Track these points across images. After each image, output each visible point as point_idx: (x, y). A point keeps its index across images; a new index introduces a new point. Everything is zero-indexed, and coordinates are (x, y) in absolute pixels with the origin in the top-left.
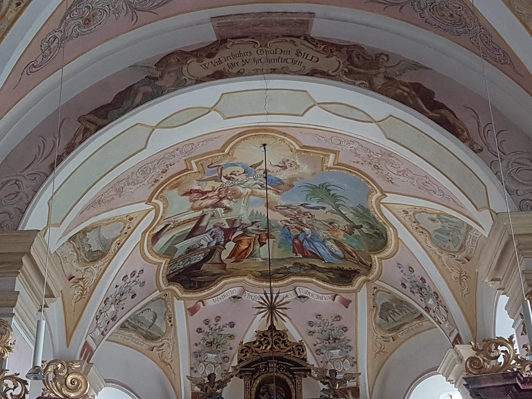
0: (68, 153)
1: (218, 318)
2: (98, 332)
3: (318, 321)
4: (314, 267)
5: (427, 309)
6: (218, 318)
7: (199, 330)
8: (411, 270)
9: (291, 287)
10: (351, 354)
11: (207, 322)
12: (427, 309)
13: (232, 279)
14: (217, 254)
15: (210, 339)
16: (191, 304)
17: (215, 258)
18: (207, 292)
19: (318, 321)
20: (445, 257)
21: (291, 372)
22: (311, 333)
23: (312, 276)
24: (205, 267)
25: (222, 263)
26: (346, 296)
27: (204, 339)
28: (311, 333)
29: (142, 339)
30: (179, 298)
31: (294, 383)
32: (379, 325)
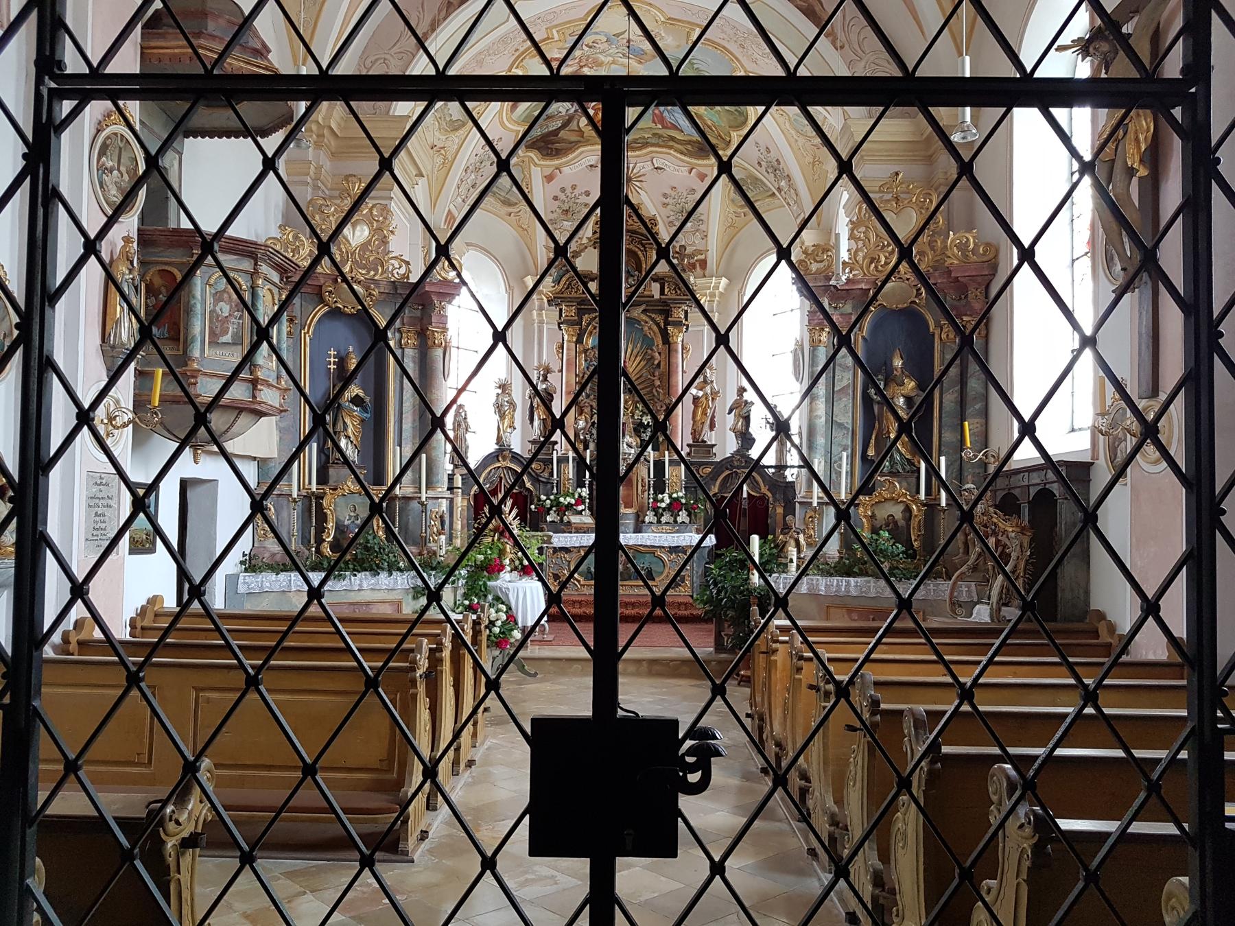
0: (433, 30)
1: (574, 187)
2: (460, 200)
3: (673, 194)
4: (672, 139)
5: (779, 189)
6: (574, 187)
7: (556, 198)
8: (768, 150)
9: (648, 158)
10: (703, 227)
11: (563, 190)
12: (779, 189)
13: (589, 148)
14: (575, 122)
15: (566, 207)
16: (548, 172)
17: (573, 125)
18: (564, 160)
19: (673, 194)
20: (801, 140)
21: (643, 245)
22: (665, 205)
23: (671, 147)
24: (562, 134)
25: (580, 130)
26: (703, 170)
27: (559, 207)
28: (665, 205)
29: (499, 205)
30: (536, 165)
31: (645, 256)
32: (733, 201)
